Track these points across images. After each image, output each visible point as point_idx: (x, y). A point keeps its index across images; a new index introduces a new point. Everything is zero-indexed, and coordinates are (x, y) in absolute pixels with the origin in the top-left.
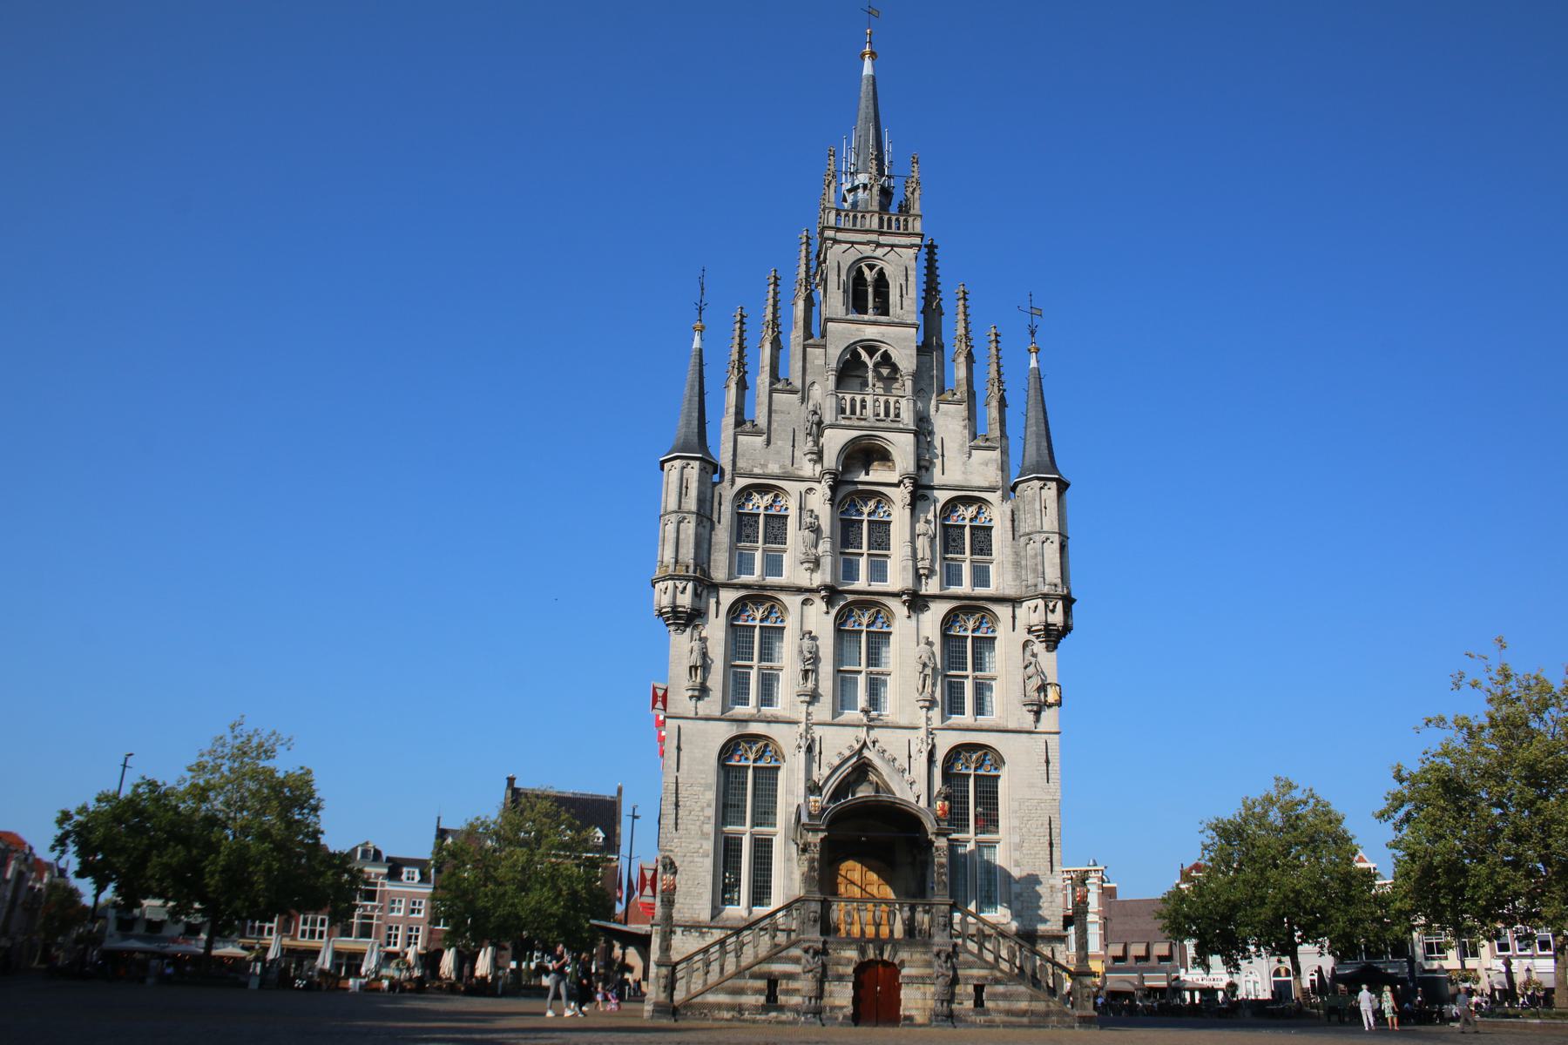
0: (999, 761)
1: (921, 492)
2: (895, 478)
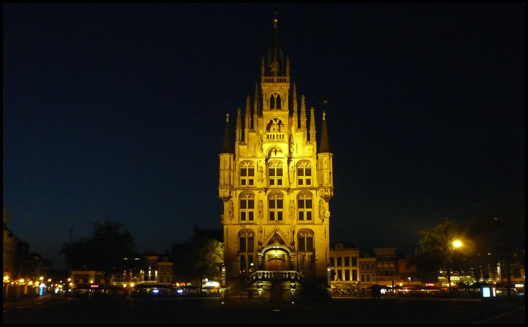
0: (312, 233)
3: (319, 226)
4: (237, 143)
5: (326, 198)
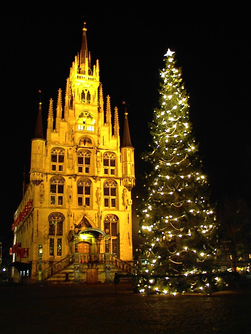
1: (98, 150)
2: (92, 147)
3: (123, 212)
4: (48, 131)
5: (128, 187)
